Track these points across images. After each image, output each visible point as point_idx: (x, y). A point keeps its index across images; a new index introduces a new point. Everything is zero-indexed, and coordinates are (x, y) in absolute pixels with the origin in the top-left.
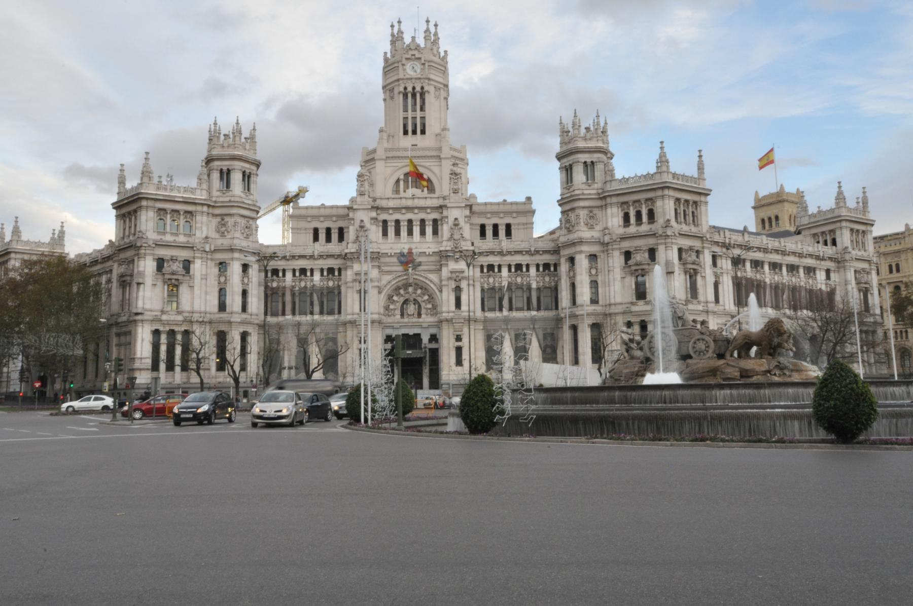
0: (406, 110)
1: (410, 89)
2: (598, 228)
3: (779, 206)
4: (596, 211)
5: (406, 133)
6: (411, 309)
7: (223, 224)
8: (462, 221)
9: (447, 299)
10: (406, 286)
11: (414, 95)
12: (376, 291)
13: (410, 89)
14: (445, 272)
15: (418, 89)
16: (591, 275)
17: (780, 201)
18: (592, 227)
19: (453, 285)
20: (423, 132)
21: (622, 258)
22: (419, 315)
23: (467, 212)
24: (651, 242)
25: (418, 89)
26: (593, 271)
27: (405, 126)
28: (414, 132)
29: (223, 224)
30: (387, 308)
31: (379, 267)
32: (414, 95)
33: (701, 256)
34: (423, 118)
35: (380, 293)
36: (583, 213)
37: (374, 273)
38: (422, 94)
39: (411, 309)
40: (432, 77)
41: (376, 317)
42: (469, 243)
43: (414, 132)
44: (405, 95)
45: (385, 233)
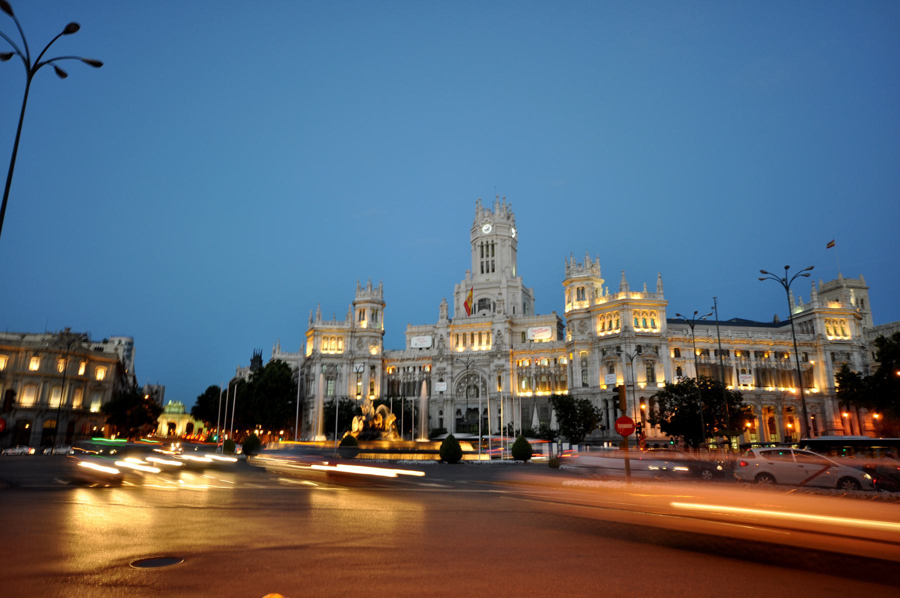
0: (482, 257)
1: (485, 243)
2: (587, 333)
3: (838, 291)
4: (586, 321)
5: (483, 272)
6: (472, 391)
7: (360, 342)
8: (503, 332)
9: (493, 384)
10: (468, 377)
11: (487, 246)
12: (450, 380)
13: (485, 243)
14: (492, 367)
15: (490, 242)
16: (582, 366)
17: (838, 288)
18: (582, 333)
19: (496, 375)
20: (493, 271)
21: (601, 354)
22: (478, 396)
23: (507, 325)
24: (617, 341)
25: (490, 242)
26: (584, 364)
27: (482, 267)
28: (488, 271)
29: (360, 342)
30: (457, 391)
31: (452, 364)
32: (487, 246)
33: (659, 351)
34: (493, 261)
35: (452, 381)
36: (576, 323)
37: (449, 369)
38: (493, 246)
39: (472, 391)
40: (498, 233)
41: (449, 397)
42: (508, 346)
43: (488, 271)
44: (482, 247)
45: (457, 343)
